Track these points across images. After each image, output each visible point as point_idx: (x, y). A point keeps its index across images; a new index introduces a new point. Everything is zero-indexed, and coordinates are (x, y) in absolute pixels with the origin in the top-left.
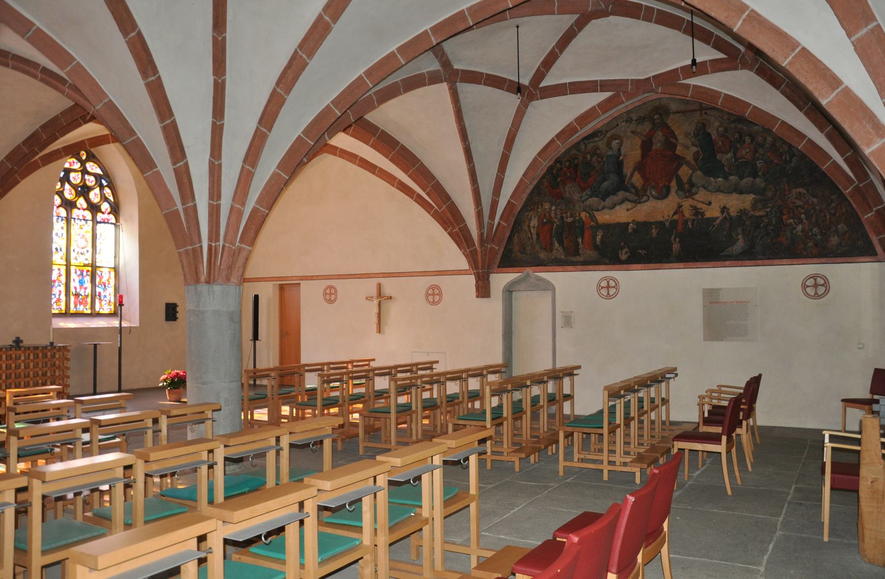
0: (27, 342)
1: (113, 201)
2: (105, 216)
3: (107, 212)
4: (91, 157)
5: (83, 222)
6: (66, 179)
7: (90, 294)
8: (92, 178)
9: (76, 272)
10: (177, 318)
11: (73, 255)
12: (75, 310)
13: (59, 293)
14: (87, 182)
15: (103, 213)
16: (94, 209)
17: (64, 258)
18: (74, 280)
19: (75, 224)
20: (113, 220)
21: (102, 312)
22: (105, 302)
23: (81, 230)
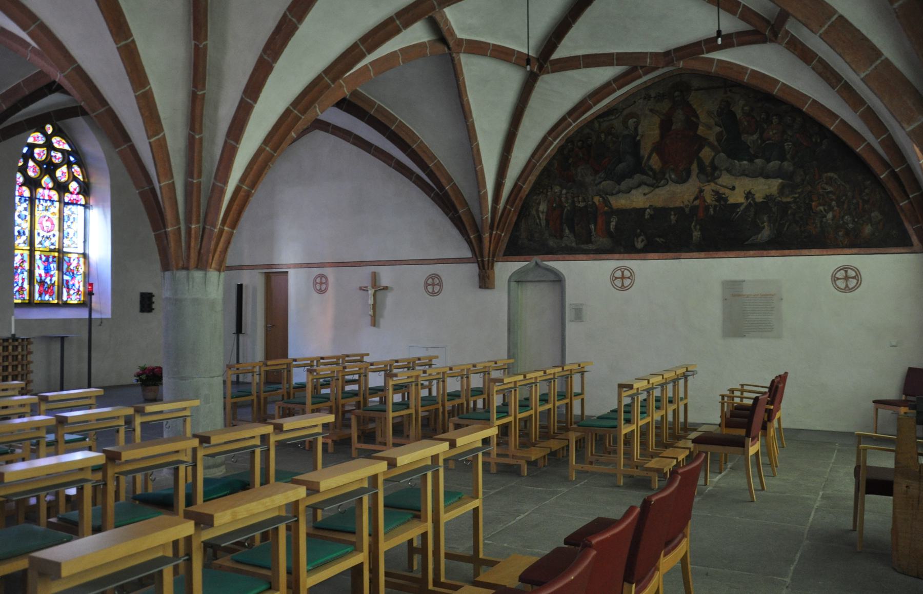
1: (82, 179)
2: (74, 196)
3: (76, 192)
4: (58, 132)
5: (49, 203)
6: (30, 155)
7: (56, 284)
8: (59, 155)
9: (41, 258)
10: (153, 309)
11: (37, 240)
12: (40, 299)
14: (54, 160)
15: (72, 193)
16: (61, 188)
17: (28, 242)
18: (39, 267)
19: (40, 206)
20: (83, 202)
23: (46, 213)
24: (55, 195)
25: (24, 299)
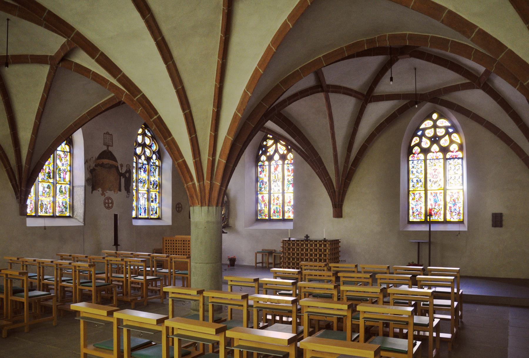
2: (454, 154)
3: (455, 151)
6: (423, 135)
13: (419, 209)
15: (452, 152)
16: (444, 150)
17: (423, 186)
19: (430, 163)
21: (452, 220)
22: (455, 213)
24: (440, 155)
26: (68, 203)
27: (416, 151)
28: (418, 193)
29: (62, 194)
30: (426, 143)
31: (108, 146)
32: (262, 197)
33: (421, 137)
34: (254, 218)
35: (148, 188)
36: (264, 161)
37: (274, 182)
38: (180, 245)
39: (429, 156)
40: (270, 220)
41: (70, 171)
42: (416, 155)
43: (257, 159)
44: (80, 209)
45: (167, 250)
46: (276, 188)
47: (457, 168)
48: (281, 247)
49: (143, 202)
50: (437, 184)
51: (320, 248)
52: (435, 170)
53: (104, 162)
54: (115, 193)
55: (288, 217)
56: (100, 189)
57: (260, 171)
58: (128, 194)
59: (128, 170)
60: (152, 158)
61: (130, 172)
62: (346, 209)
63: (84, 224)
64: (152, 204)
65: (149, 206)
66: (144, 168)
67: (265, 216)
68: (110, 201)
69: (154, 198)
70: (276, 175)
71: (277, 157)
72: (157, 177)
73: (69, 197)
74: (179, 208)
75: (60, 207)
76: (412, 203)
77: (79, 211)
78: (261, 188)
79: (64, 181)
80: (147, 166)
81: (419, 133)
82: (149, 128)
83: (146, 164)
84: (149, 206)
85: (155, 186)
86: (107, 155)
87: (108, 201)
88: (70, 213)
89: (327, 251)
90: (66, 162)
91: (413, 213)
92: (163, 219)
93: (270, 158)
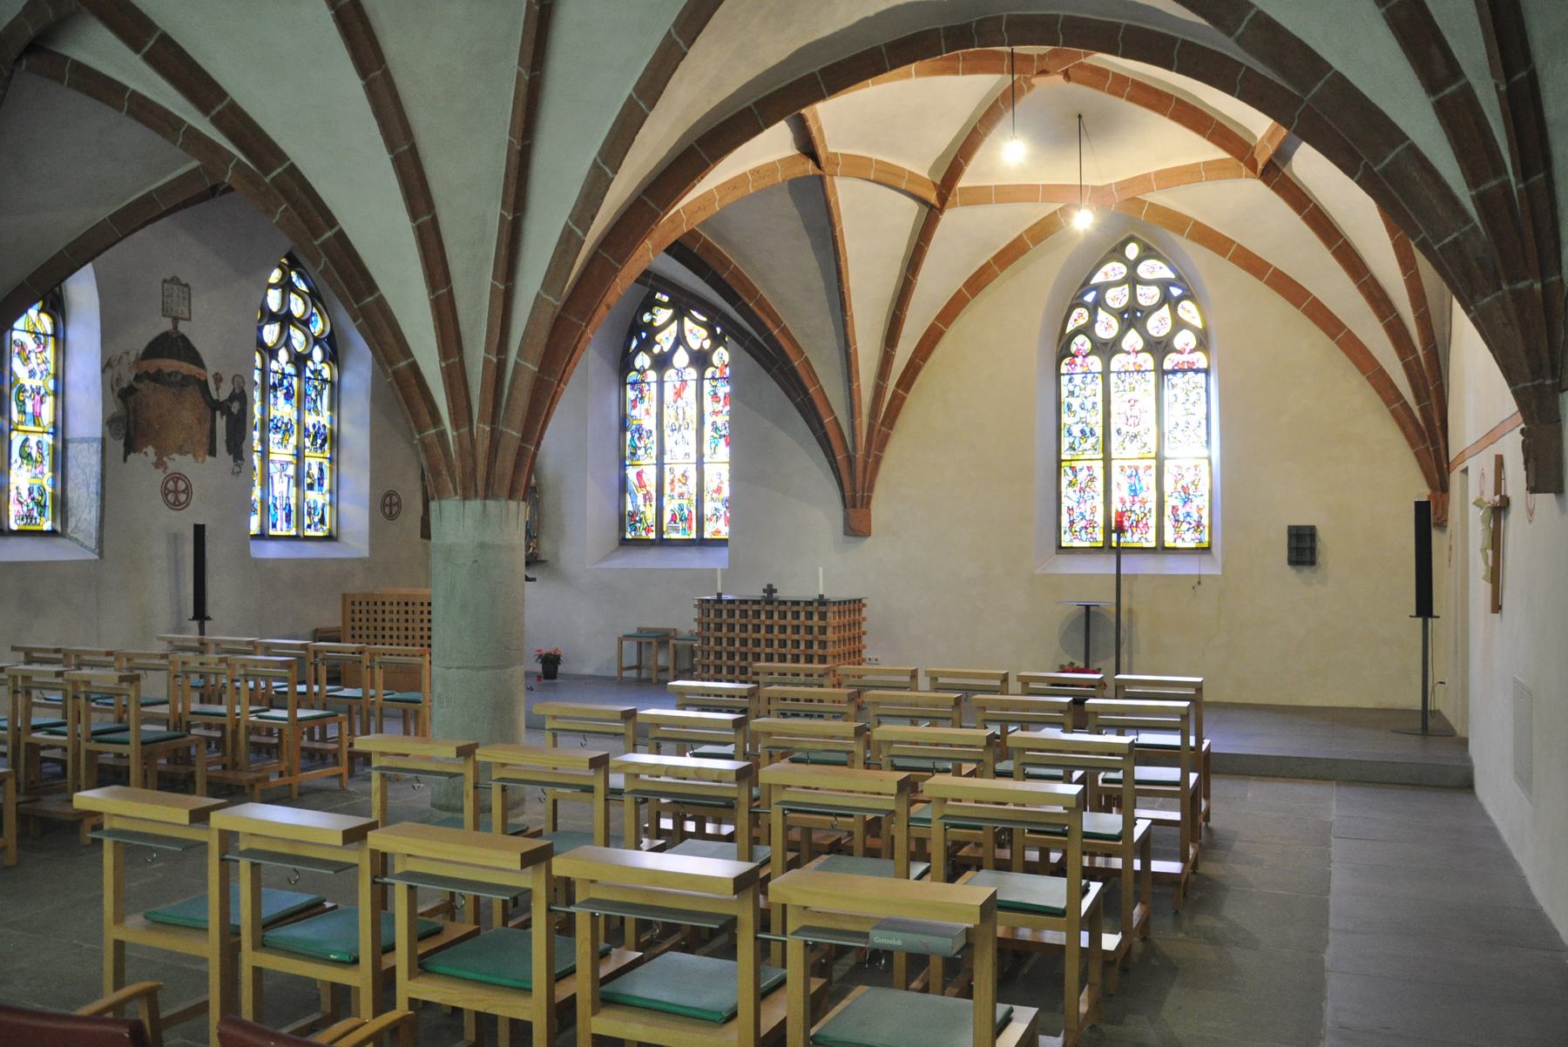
0: (782, 594)
3: (1188, 351)
4: (1148, 252)
6: (1099, 303)
11: (1115, 440)
13: (1089, 511)
15: (1180, 352)
16: (1159, 347)
17: (1100, 446)
19: (1120, 382)
21: (1180, 544)
22: (1188, 526)
24: (1147, 360)
25: (1095, 540)
26: (49, 490)
27: (1080, 347)
28: (1085, 469)
29: (31, 463)
30: (1107, 327)
31: (176, 320)
32: (639, 475)
33: (1093, 309)
34: (614, 535)
35: (297, 447)
36: (645, 371)
37: (673, 430)
38: (395, 616)
39: (1117, 362)
40: (661, 542)
41: (55, 393)
42: (1081, 357)
43: (625, 364)
44: (87, 511)
45: (357, 632)
46: (680, 449)
47: (1193, 396)
48: (695, 620)
49: (282, 487)
50: (1137, 444)
51: (810, 623)
52: (1132, 402)
53: (163, 368)
54: (196, 461)
55: (713, 533)
56: (150, 450)
57: (633, 398)
58: (239, 466)
59: (237, 391)
60: (309, 356)
61: (241, 397)
62: (880, 509)
63: (101, 554)
64: (311, 496)
65: (300, 499)
66: (287, 388)
67: (648, 530)
68: (182, 485)
69: (316, 477)
70: (680, 412)
71: (681, 358)
72: (327, 414)
73: (50, 474)
74: (391, 505)
75: (21, 503)
76: (1069, 497)
77: (85, 515)
78: (636, 448)
79: (34, 423)
80: (295, 381)
81: (1089, 298)
82: (303, 267)
83: (290, 375)
84: (300, 499)
85: (319, 441)
86: (173, 345)
87: (176, 484)
88: (54, 520)
89: (829, 631)
90: (43, 367)
91: (1072, 523)
92: (344, 538)
93: (662, 362)
